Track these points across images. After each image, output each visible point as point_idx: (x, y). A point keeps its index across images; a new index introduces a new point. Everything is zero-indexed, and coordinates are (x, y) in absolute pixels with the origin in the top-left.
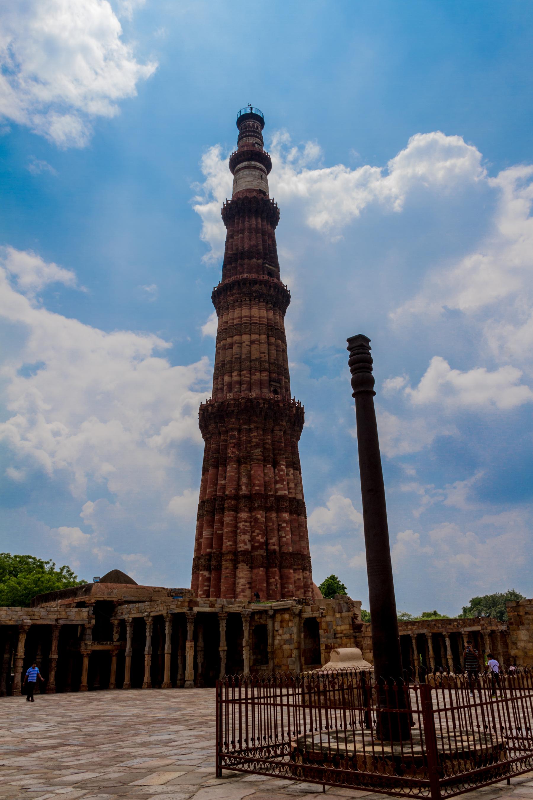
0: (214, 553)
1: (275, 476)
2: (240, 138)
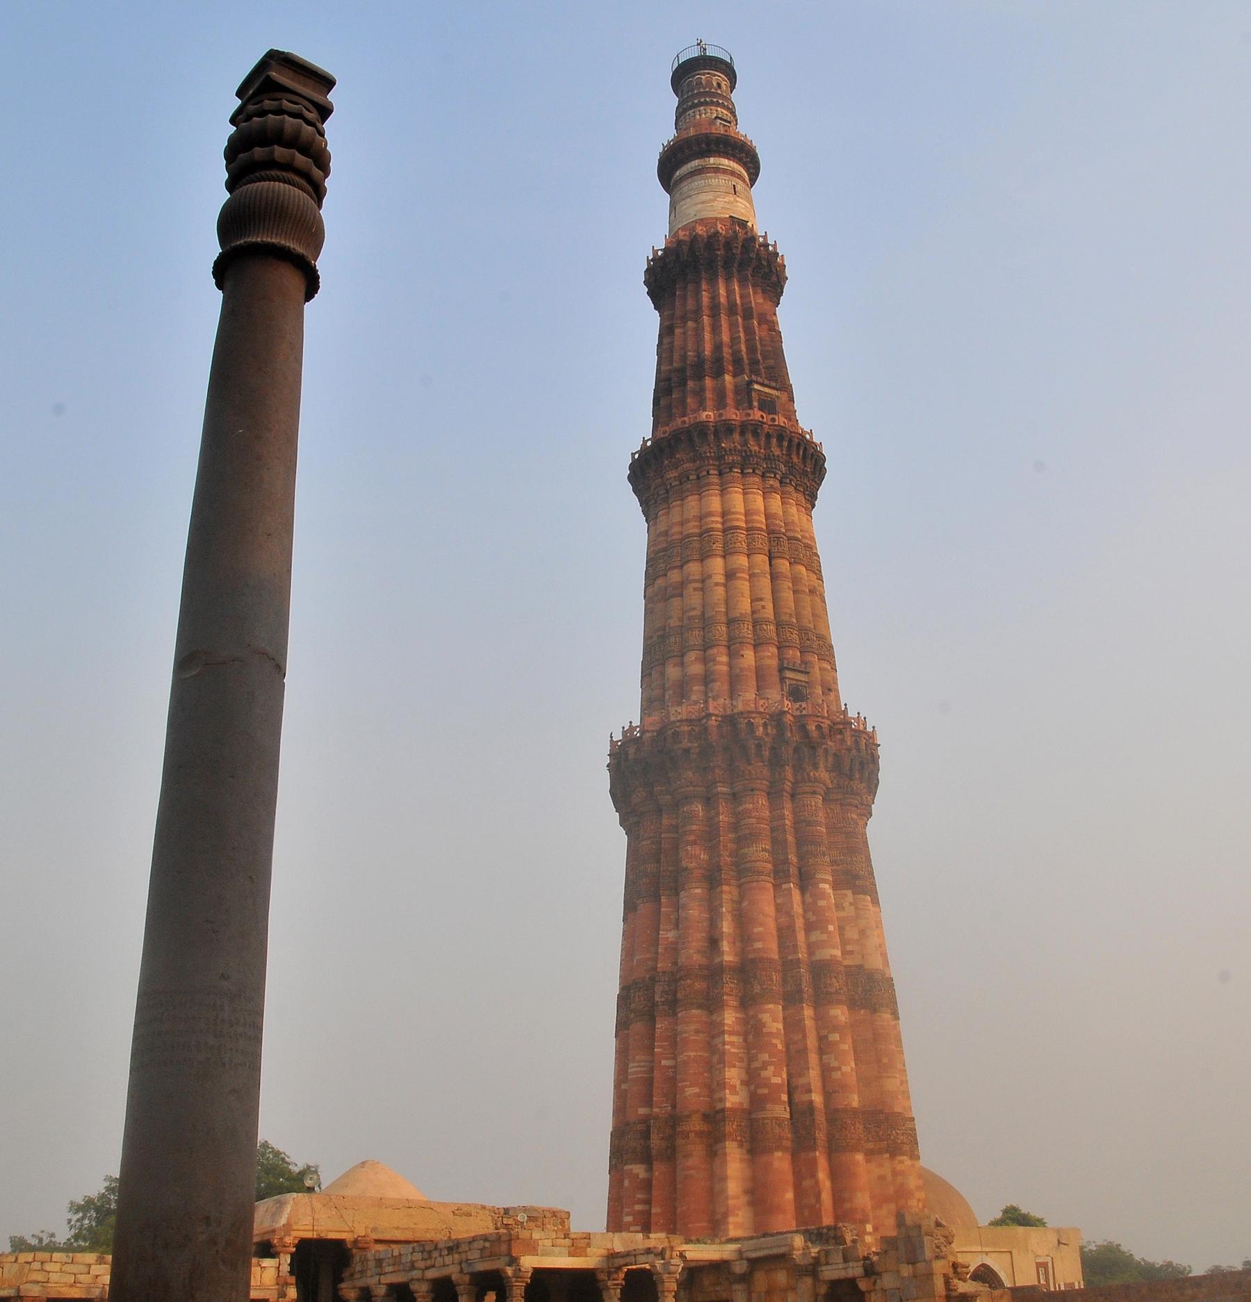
0: (656, 1118)
1: (805, 911)
2: (681, 113)
